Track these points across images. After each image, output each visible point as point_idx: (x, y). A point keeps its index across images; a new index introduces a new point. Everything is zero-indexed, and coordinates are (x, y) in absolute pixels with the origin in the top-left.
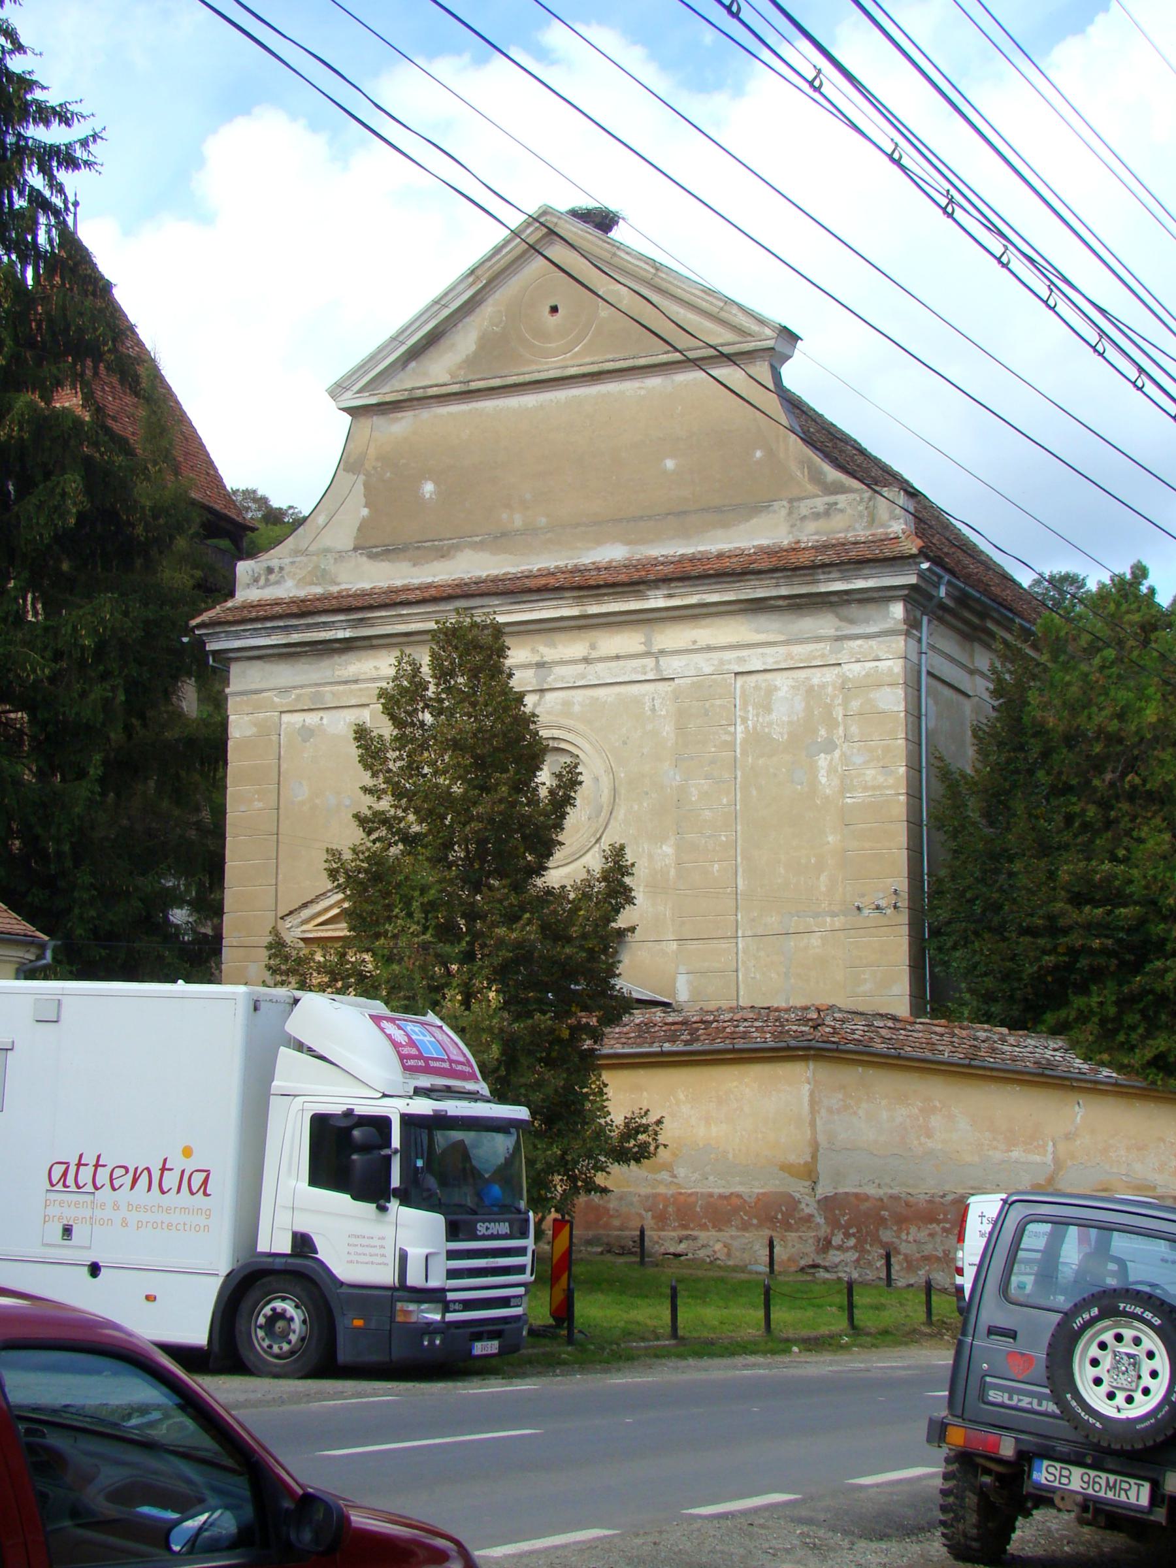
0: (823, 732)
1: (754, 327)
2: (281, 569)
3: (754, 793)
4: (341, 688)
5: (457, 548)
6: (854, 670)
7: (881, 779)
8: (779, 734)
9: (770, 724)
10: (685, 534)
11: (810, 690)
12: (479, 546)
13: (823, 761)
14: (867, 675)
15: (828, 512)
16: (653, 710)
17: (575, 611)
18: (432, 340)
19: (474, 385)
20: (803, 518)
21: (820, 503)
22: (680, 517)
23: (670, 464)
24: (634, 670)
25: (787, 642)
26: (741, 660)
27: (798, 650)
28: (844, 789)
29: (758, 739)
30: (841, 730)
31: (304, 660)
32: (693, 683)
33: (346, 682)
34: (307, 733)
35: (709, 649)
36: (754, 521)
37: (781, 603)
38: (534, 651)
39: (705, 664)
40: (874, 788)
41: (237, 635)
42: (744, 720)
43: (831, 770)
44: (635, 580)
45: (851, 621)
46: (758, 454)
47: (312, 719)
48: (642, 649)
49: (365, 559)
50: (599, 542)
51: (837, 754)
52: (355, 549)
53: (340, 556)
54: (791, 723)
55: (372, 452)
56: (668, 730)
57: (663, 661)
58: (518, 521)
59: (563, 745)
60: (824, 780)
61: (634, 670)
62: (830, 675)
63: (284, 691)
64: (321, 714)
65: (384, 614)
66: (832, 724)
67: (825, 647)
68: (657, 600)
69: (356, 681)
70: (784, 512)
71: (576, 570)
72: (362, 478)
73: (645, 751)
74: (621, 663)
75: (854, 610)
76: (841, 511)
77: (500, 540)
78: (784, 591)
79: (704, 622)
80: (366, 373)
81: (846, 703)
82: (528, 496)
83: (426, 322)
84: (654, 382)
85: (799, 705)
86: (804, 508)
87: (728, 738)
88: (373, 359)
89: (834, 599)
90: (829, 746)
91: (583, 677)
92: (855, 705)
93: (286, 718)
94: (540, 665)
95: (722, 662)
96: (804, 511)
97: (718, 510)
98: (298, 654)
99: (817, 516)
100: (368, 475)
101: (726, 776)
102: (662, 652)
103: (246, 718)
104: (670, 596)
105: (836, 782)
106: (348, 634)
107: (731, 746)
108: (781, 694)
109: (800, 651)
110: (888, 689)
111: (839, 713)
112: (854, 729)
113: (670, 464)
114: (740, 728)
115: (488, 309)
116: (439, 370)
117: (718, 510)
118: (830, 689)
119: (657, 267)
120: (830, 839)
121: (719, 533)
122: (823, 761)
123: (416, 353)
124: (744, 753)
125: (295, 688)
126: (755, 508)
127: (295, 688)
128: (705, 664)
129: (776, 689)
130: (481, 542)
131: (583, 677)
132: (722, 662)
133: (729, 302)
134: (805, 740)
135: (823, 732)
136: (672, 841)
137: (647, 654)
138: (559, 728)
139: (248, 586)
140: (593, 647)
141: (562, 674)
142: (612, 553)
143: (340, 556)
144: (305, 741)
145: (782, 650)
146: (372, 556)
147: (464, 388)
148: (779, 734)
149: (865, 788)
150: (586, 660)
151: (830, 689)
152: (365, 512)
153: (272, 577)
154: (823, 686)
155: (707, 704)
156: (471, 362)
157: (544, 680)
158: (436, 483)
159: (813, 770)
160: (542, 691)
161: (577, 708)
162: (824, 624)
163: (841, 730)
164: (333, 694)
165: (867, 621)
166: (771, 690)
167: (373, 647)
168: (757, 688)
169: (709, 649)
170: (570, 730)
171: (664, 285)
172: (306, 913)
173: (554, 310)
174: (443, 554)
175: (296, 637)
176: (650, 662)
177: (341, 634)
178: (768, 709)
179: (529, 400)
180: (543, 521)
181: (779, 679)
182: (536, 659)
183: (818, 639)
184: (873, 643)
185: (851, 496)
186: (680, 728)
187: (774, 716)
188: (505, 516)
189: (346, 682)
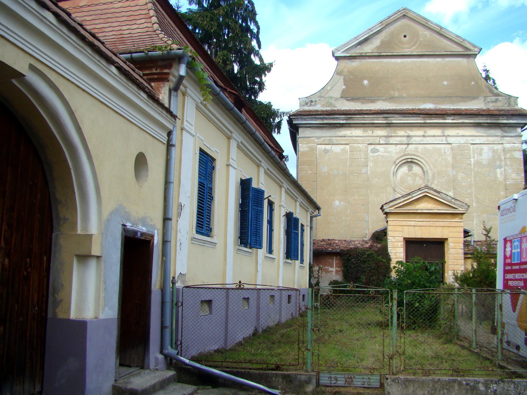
0: (498, 163)
1: (472, 48)
2: (316, 101)
3: (478, 179)
4: (339, 138)
5: (377, 100)
6: (507, 146)
7: (517, 177)
8: (485, 162)
9: (482, 159)
10: (452, 103)
11: (494, 151)
12: (385, 100)
13: (498, 171)
14: (511, 148)
15: (496, 101)
16: (445, 152)
17: (422, 122)
18: (366, 40)
19: (382, 54)
20: (489, 102)
21: (494, 98)
22: (450, 98)
23: (445, 83)
24: (439, 140)
25: (487, 136)
26: (473, 140)
27: (490, 138)
28: (505, 179)
29: (478, 163)
30: (503, 162)
31: (325, 129)
32: (458, 146)
33: (341, 137)
34: (326, 151)
35: (463, 136)
36: (473, 101)
37: (486, 125)
38: (406, 132)
39: (462, 140)
40: (514, 179)
41: (305, 119)
42: (474, 157)
43: (501, 174)
44: (443, 114)
45: (506, 132)
46: (473, 83)
47: (328, 147)
48: (441, 134)
49: (345, 101)
50: (425, 102)
51: (503, 169)
52: (341, 97)
53: (336, 99)
54: (488, 159)
55: (345, 70)
56: (450, 158)
57: (448, 138)
58: (397, 94)
59: (415, 161)
60: (499, 176)
61: (439, 140)
62: (500, 147)
63: (318, 138)
64: (331, 146)
65: (358, 116)
66: (501, 160)
67: (499, 139)
68: (449, 121)
69: (345, 137)
70: (482, 100)
71: (419, 109)
72: (342, 77)
73: (443, 164)
74: (435, 138)
75: (506, 129)
76: (500, 101)
77: (391, 99)
78: (489, 121)
79: (461, 128)
80: (345, 47)
81: (505, 155)
82: (400, 87)
83: (366, 35)
84: (439, 60)
85: (491, 154)
86: (489, 99)
87: (469, 162)
88: (348, 43)
89: (502, 125)
90: (500, 167)
91: (422, 141)
92: (508, 156)
93: (319, 146)
94: (408, 136)
95: (467, 140)
96: (489, 100)
97: (461, 97)
98: (324, 127)
99: (493, 102)
100: (345, 76)
101: (470, 173)
102: (448, 136)
103: (305, 145)
104: (453, 119)
105: (503, 177)
106: (344, 122)
107: (470, 164)
108: (484, 151)
109: (491, 139)
110: (518, 152)
111: (503, 157)
112: (508, 162)
113: (445, 83)
114: (472, 160)
115: (383, 34)
116: (367, 49)
117: (461, 97)
118: (500, 151)
119: (441, 28)
120: (502, 193)
121: (463, 104)
122: (498, 171)
123: (360, 43)
124: (474, 167)
125: (323, 137)
126: (474, 98)
127: (323, 137)
128: (462, 140)
129: (483, 149)
130: (385, 99)
131: (422, 141)
132: (467, 140)
133: (464, 40)
134: (493, 164)
135: (498, 163)
136: (452, 191)
137: (444, 136)
138: (414, 155)
139: (304, 105)
140: (425, 132)
141: (415, 140)
142: (429, 106)
143: (336, 99)
144: (325, 153)
145: (485, 138)
146: (347, 100)
147: (379, 54)
148: (485, 162)
149: (512, 179)
150: (424, 136)
151: (500, 151)
152: (344, 87)
153: (312, 104)
154: (498, 149)
155: (463, 152)
156: (378, 48)
157: (409, 141)
158: (368, 81)
159: (496, 173)
160: (408, 144)
161: (420, 150)
162: (498, 132)
163: (503, 162)
164: (336, 140)
165: (510, 132)
166: (482, 150)
167: (350, 127)
168: (477, 148)
169: (463, 136)
170: (418, 156)
171: (443, 33)
172: (391, 204)
173: (405, 36)
174: (373, 101)
175: (325, 121)
176: (444, 138)
177: (342, 122)
178: (481, 154)
179: (399, 60)
180: (405, 95)
181: (484, 147)
182: (407, 134)
183: (497, 136)
184: (513, 139)
185: (503, 97)
186: (454, 158)
187: (483, 157)
188: (392, 92)
189: (341, 137)
